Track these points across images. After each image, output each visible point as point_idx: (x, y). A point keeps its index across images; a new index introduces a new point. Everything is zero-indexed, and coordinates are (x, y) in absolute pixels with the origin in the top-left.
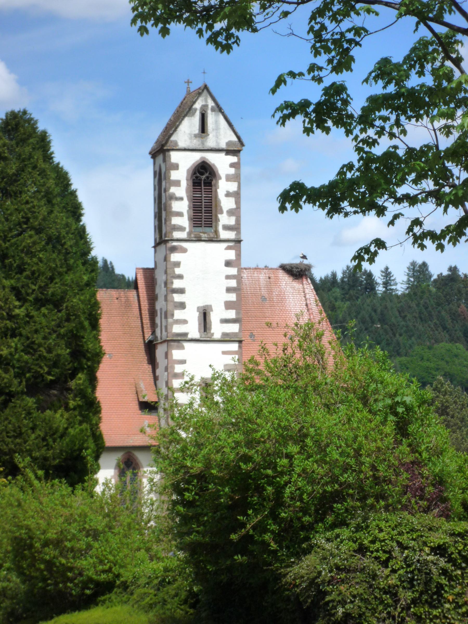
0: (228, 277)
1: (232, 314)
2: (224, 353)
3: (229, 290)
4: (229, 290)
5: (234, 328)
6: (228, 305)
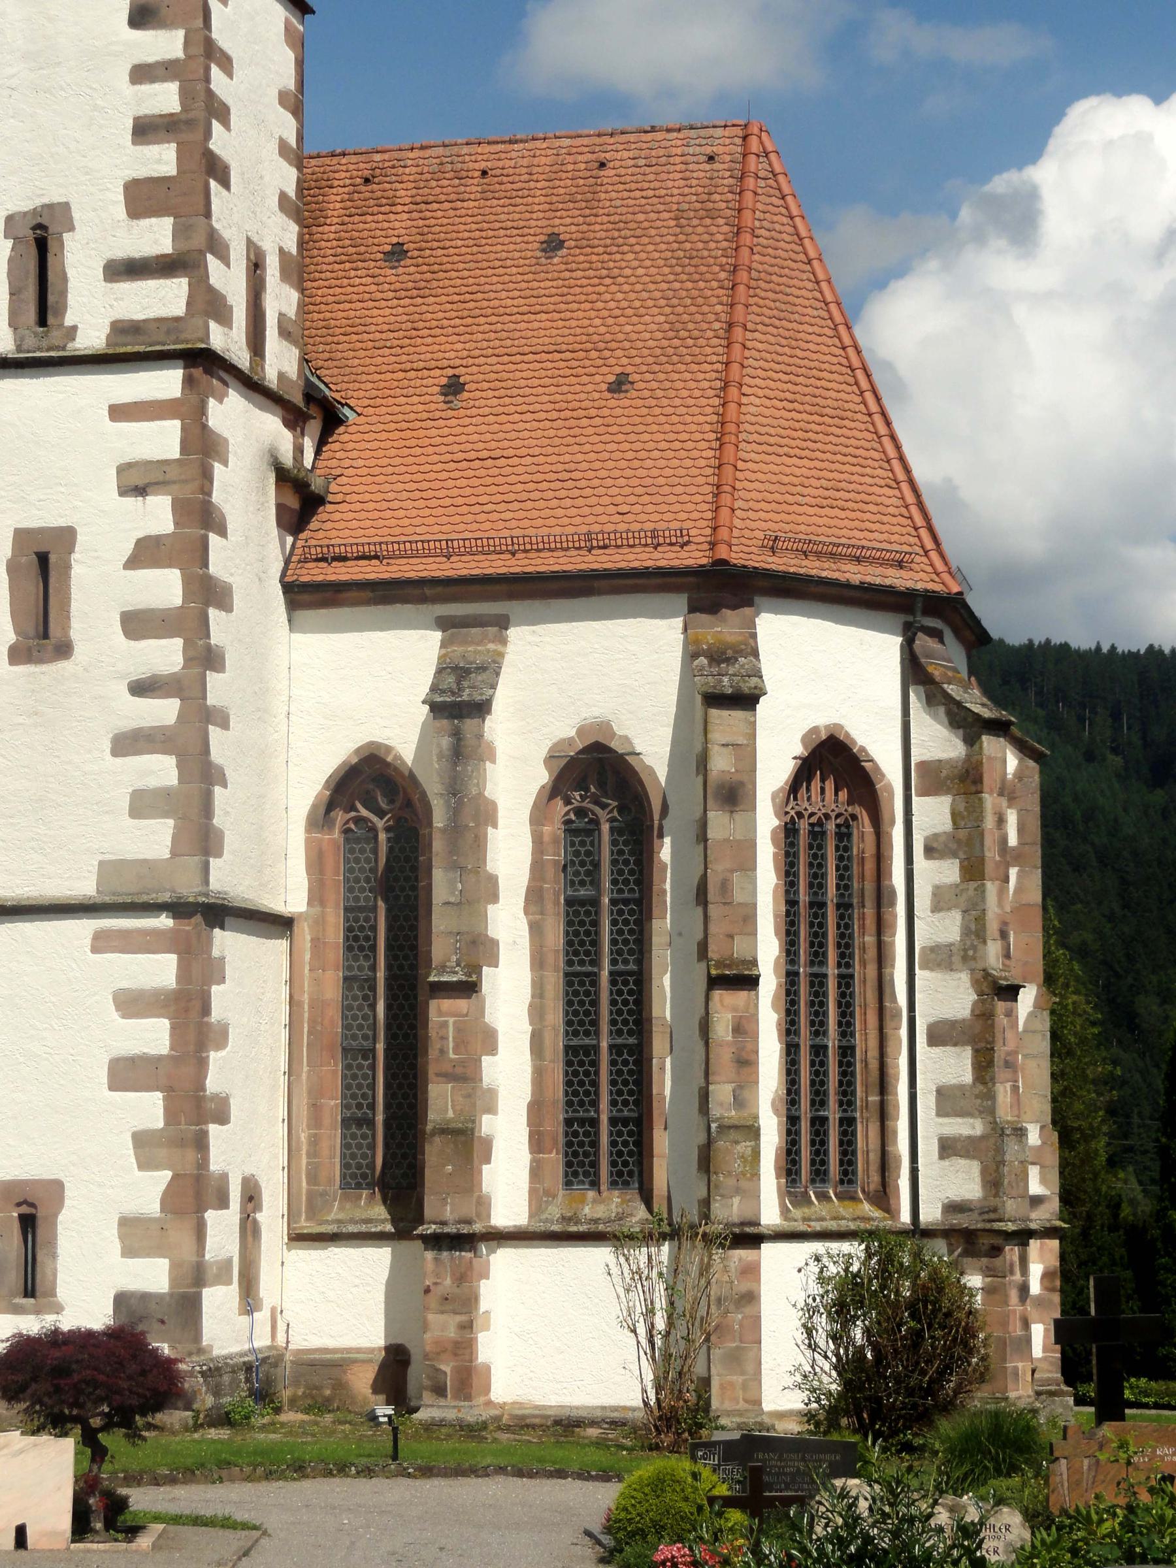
0: (142, 74)
1: (156, 236)
2: (119, 412)
3: (146, 130)
4: (146, 130)
5: (166, 298)
6: (143, 198)
